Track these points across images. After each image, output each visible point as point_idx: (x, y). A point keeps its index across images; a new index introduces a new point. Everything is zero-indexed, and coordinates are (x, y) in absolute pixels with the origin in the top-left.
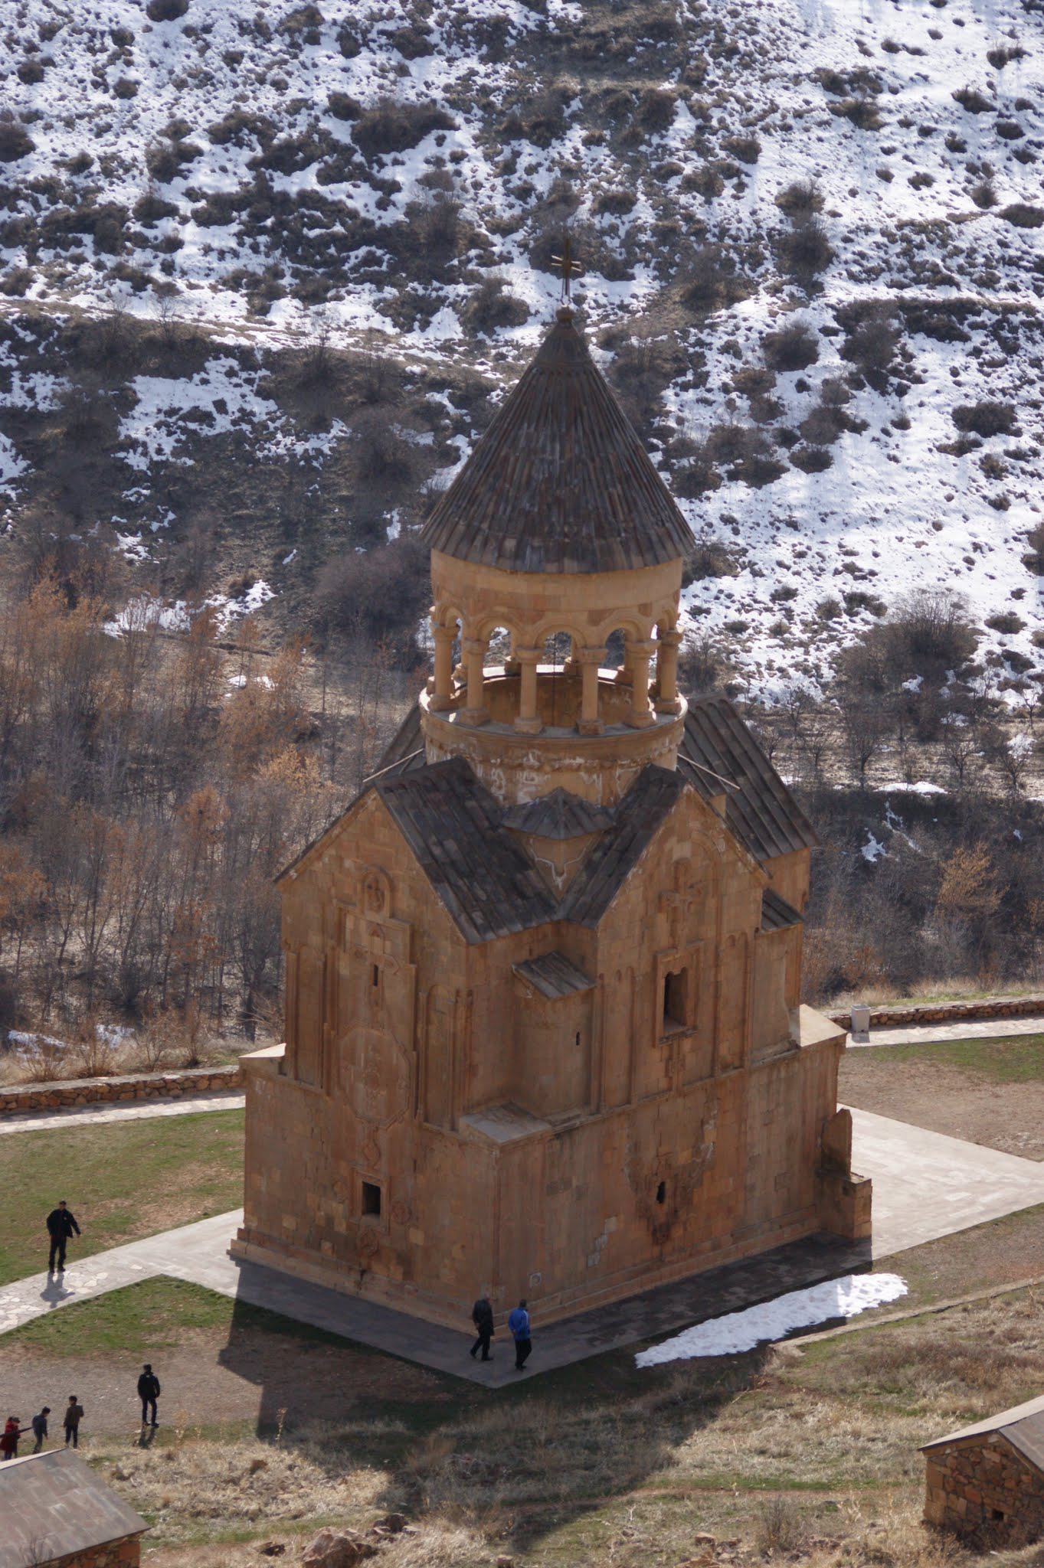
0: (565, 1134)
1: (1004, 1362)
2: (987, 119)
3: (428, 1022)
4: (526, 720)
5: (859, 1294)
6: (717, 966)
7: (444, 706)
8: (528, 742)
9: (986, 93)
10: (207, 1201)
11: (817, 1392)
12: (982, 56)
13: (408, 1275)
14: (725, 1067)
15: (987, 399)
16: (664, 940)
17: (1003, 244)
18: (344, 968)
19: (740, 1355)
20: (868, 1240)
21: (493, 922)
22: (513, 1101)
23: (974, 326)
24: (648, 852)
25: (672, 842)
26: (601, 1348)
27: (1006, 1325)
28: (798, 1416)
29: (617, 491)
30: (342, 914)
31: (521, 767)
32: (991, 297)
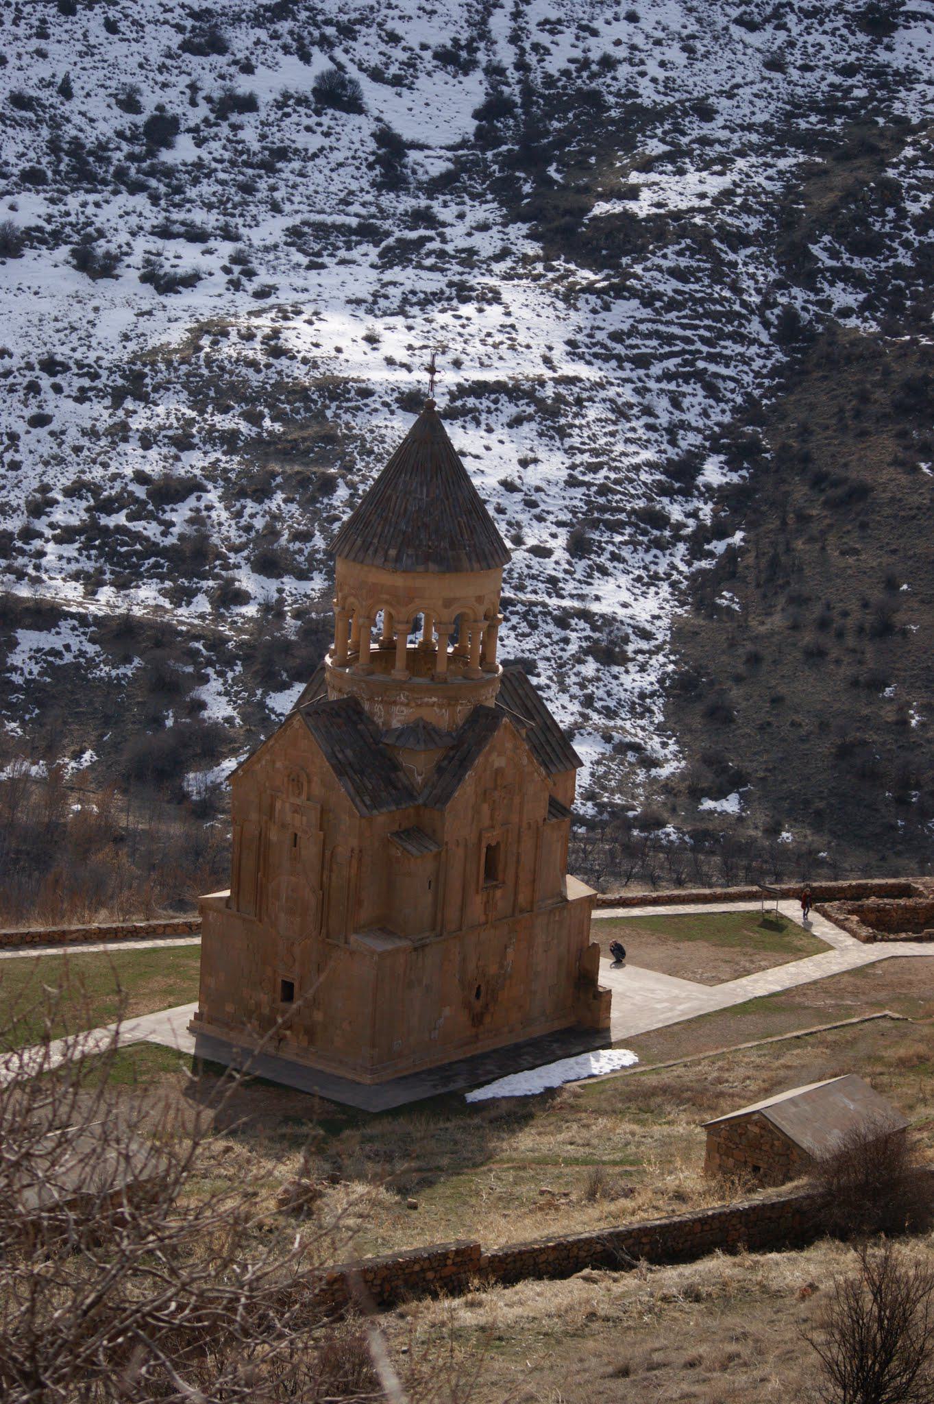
0: (420, 948)
1: (721, 1095)
2: (518, 496)
3: (331, 870)
4: (399, 672)
5: (605, 1062)
6: (519, 842)
7: (343, 663)
8: (400, 686)
9: (518, 482)
10: (173, 998)
11: (599, 1112)
12: (515, 461)
13: (311, 1042)
14: (521, 911)
15: (520, 655)
16: (487, 823)
17: (529, 567)
18: (274, 836)
19: (534, 1096)
20: (608, 1029)
21: (376, 804)
22: (385, 926)
23: (512, 613)
24: (479, 761)
25: (494, 755)
26: (441, 1090)
27: (715, 1074)
28: (587, 1126)
29: (463, 520)
30: (273, 798)
31: (395, 703)
32: (522, 596)
